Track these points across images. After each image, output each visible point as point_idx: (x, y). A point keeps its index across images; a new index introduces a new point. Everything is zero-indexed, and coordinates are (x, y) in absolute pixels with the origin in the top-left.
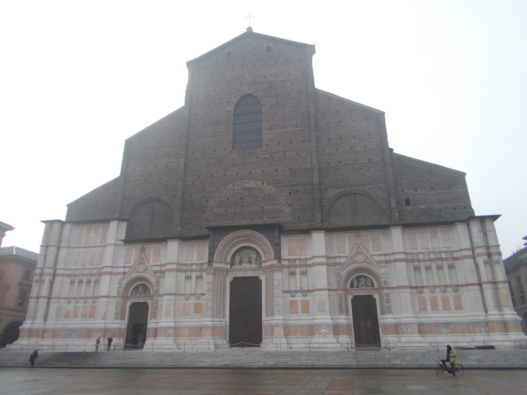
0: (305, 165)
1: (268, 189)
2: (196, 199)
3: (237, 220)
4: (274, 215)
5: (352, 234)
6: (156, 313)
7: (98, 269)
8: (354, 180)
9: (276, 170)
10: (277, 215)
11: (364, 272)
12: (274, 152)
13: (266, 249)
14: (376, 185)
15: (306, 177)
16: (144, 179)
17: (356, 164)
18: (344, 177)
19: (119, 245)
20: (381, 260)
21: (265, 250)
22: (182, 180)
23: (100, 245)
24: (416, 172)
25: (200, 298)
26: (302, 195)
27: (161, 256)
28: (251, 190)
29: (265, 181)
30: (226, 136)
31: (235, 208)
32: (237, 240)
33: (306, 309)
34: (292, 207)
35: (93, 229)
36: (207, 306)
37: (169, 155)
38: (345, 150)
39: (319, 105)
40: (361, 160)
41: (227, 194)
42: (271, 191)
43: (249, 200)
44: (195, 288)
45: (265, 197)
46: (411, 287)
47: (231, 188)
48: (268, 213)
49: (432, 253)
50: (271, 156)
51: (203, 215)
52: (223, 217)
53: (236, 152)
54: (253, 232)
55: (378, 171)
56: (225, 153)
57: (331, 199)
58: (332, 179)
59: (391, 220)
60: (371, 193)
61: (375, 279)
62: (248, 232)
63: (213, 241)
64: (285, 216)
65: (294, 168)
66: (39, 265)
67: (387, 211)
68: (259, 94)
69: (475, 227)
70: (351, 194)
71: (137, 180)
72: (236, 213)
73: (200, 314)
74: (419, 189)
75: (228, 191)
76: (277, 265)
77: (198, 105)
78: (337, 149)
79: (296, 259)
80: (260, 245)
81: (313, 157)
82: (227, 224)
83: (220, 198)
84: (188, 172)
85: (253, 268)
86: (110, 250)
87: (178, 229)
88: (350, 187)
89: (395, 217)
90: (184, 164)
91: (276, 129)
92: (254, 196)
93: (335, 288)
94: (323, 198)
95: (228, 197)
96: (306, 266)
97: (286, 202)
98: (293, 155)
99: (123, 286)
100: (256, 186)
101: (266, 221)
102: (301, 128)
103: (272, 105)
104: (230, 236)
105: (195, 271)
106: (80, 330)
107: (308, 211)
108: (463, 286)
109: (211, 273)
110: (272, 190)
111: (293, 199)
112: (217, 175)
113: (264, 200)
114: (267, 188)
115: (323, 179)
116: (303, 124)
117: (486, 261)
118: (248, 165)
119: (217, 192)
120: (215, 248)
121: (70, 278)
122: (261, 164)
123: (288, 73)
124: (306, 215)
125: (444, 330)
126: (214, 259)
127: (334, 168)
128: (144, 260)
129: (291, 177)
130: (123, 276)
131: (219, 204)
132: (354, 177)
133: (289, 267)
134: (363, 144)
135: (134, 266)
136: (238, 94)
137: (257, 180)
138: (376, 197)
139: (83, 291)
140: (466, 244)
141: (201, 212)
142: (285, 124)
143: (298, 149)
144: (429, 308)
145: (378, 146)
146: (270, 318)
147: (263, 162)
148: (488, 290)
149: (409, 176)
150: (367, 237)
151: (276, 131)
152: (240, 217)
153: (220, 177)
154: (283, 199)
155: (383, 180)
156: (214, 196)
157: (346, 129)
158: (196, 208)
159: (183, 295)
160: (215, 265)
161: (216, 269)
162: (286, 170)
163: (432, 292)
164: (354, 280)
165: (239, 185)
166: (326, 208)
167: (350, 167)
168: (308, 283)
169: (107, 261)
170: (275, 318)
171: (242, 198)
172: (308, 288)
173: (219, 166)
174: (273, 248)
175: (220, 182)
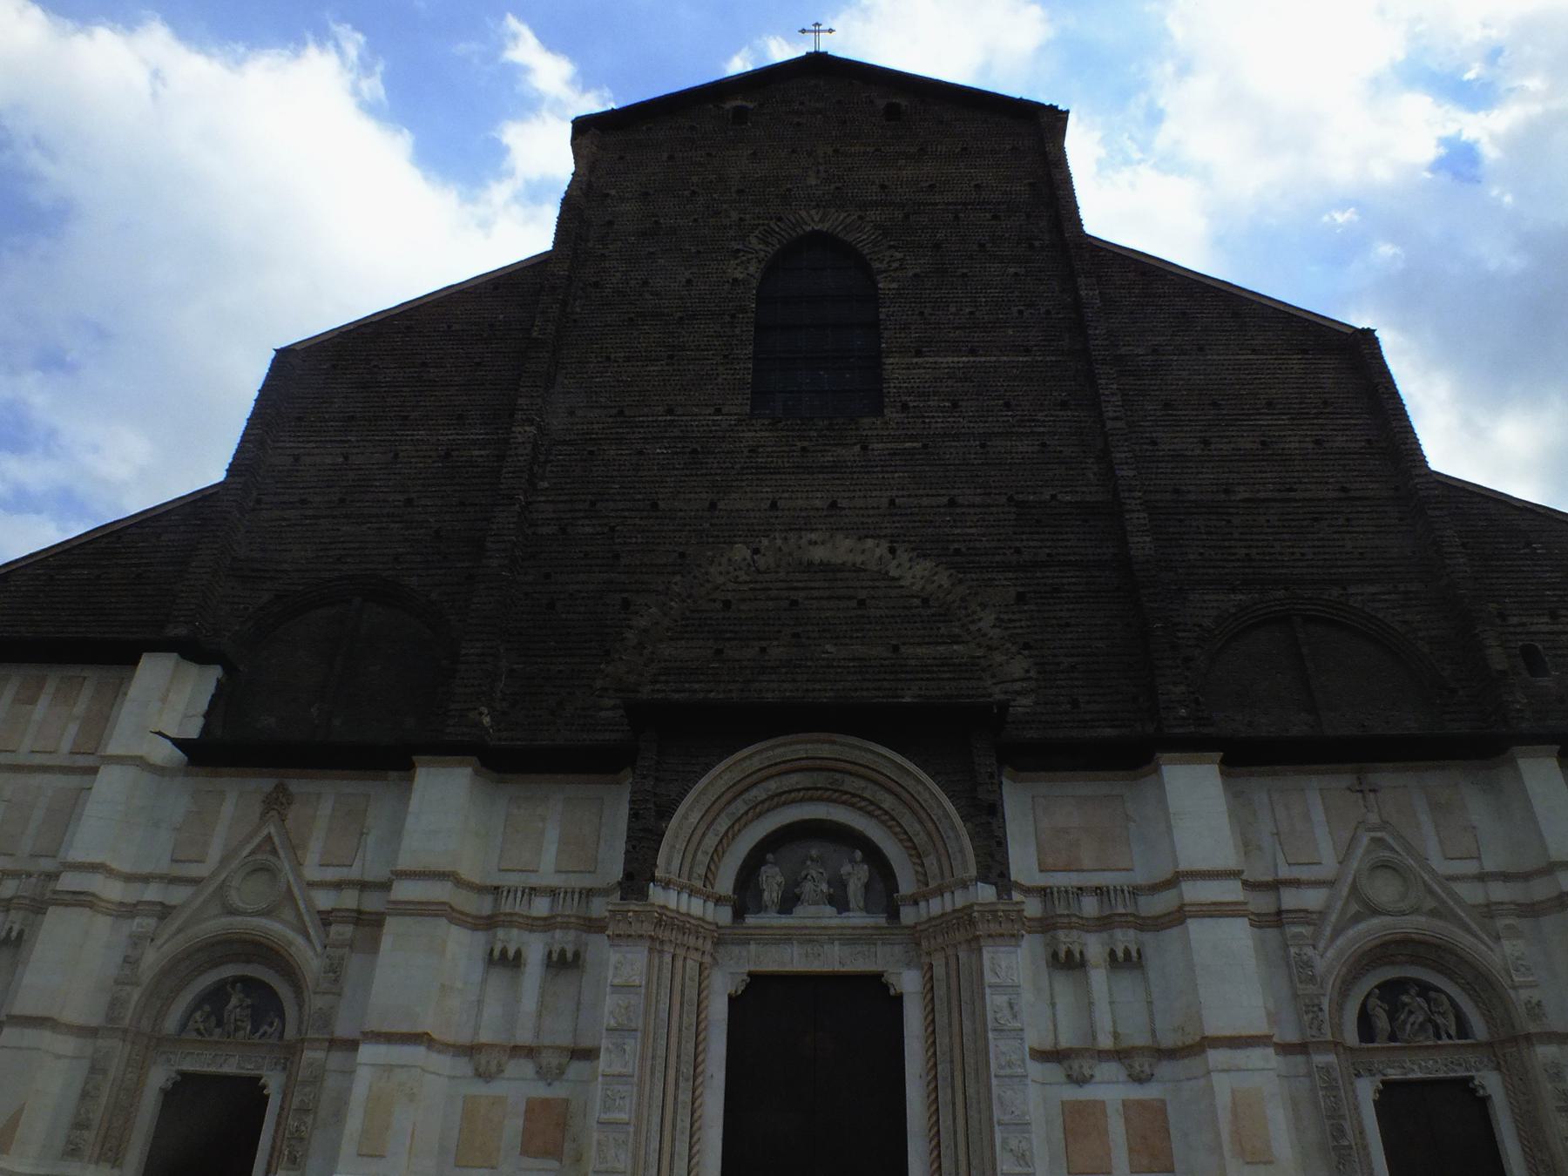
0: (1078, 489)
1: (915, 573)
2: (571, 594)
6: (302, 1139)
7: (33, 880)
8: (1294, 560)
9: (952, 503)
11: (1415, 960)
13: (929, 834)
17: (1295, 500)
18: (1250, 547)
21: (921, 839)
23: (66, 763)
24: (1536, 549)
25: (561, 1071)
28: (839, 575)
29: (904, 542)
31: (764, 644)
32: (773, 785)
34: (1036, 652)
35: (50, 688)
36: (604, 1117)
41: (724, 584)
42: (933, 582)
44: (540, 1015)
45: (905, 607)
47: (745, 559)
48: (921, 676)
50: (925, 446)
52: (701, 682)
54: (860, 748)
56: (719, 425)
58: (1202, 551)
60: (1380, 616)
64: (1006, 693)
65: (1031, 497)
71: (303, 502)
73: (555, 1164)
75: (728, 573)
79: (1080, 889)
80: (893, 819)
81: (1118, 455)
85: (854, 928)
88: (1286, 589)
90: (529, 447)
92: (854, 598)
93: (1292, 1037)
95: (729, 596)
98: (1021, 449)
100: (859, 559)
102: (1048, 359)
103: (916, 275)
104: (744, 759)
105: (546, 924)
109: (641, 936)
110: (936, 578)
113: (898, 620)
114: (910, 568)
118: (821, 476)
119: (674, 573)
120: (666, 812)
126: (655, 865)
127: (1204, 510)
128: (274, 852)
132: (1295, 550)
134: (1309, 433)
135: (223, 877)
137: (867, 537)
143: (1042, 429)
145: (1369, 441)
147: (889, 469)
149: (1515, 560)
151: (940, 360)
152: (786, 685)
154: (987, 620)
159: (470, 1051)
160: (656, 895)
161: (666, 920)
162: (997, 506)
164: (1373, 1001)
165: (780, 549)
167: (1272, 511)
168: (1151, 1015)
171: (794, 603)
172: (1153, 1032)
173: (688, 472)
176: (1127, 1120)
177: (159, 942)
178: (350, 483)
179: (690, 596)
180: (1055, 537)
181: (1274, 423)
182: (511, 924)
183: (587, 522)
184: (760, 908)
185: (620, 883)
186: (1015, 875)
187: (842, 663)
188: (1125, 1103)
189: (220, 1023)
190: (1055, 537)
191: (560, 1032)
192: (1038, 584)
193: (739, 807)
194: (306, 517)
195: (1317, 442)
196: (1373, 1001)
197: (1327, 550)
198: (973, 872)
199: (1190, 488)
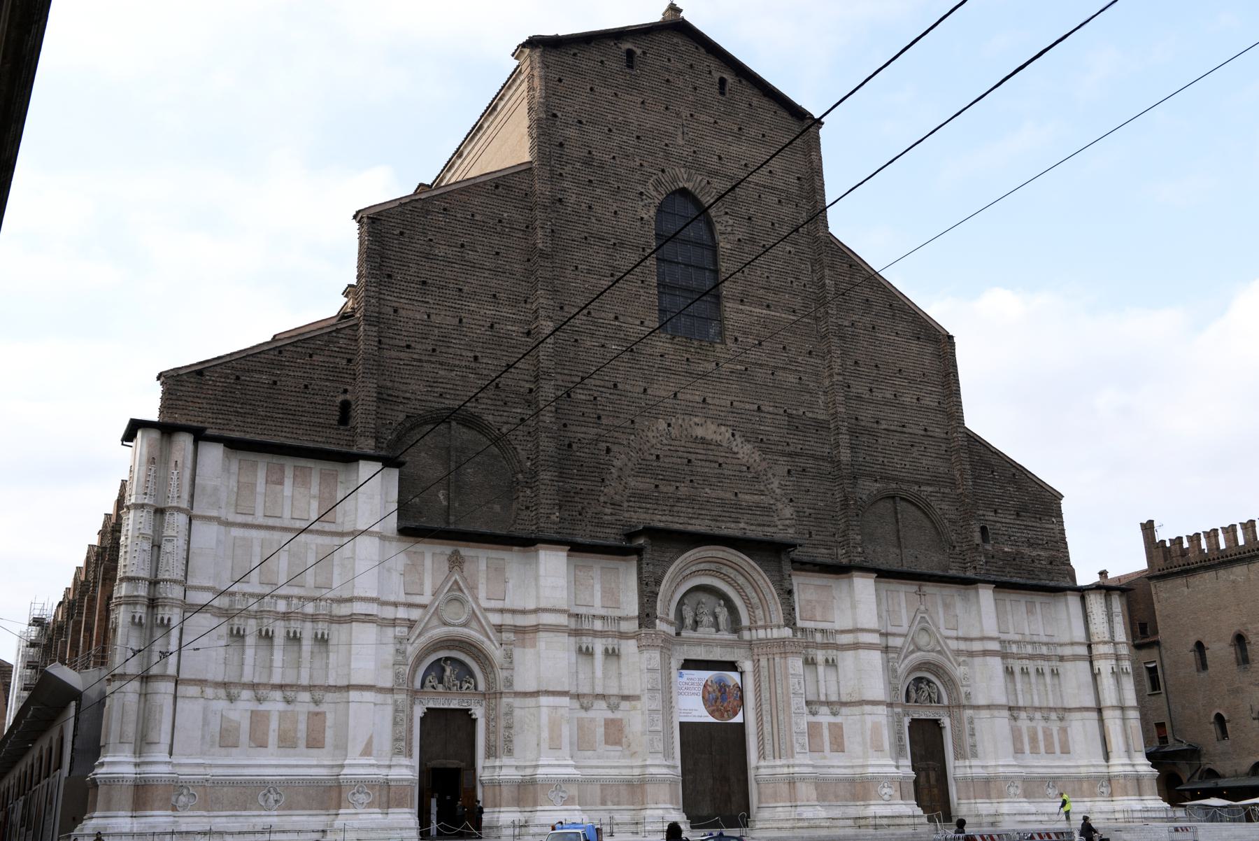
3: (682, 515)
5: (912, 587)
10: (766, 518)
11: (928, 670)
12: (753, 364)
16: (430, 348)
17: (905, 433)
20: (960, 648)
21: (755, 600)
26: (813, 481)
27: (510, 585)
28: (710, 447)
31: (678, 484)
33: (838, 744)
35: (289, 472)
36: (651, 729)
38: (885, 396)
43: (706, 470)
48: (747, 511)
50: (746, 369)
51: (602, 488)
53: (669, 336)
54: (735, 555)
62: (725, 554)
65: (794, 412)
67: (957, 548)
73: (620, 748)
74: (1000, 511)
75: (657, 437)
77: (564, 175)
78: (871, 390)
83: (640, 449)
91: (753, 305)
93: (888, 701)
99: (410, 661)
100: (719, 438)
103: (739, 240)
107: (826, 521)
111: (796, 488)
112: (628, 387)
114: (742, 447)
120: (658, 582)
122: (727, 385)
124: (822, 529)
125: (1050, 790)
128: (461, 590)
130: (406, 630)
131: (639, 466)
135: (436, 604)
140: (1080, 635)
141: (597, 479)
143: (801, 369)
144: (1027, 748)
145: (939, 403)
151: (753, 309)
152: (689, 510)
153: (636, 395)
158: (582, 465)
159: (578, 696)
168: (838, 686)
169: (366, 585)
170: (797, 762)
171: (689, 461)
172: (839, 694)
173: (630, 365)
176: (830, 731)
177: (411, 641)
178: (436, 338)
182: (586, 635)
183: (582, 392)
187: (713, 500)
188: (829, 723)
195: (918, 399)
196: (911, 687)
199: (864, 418)
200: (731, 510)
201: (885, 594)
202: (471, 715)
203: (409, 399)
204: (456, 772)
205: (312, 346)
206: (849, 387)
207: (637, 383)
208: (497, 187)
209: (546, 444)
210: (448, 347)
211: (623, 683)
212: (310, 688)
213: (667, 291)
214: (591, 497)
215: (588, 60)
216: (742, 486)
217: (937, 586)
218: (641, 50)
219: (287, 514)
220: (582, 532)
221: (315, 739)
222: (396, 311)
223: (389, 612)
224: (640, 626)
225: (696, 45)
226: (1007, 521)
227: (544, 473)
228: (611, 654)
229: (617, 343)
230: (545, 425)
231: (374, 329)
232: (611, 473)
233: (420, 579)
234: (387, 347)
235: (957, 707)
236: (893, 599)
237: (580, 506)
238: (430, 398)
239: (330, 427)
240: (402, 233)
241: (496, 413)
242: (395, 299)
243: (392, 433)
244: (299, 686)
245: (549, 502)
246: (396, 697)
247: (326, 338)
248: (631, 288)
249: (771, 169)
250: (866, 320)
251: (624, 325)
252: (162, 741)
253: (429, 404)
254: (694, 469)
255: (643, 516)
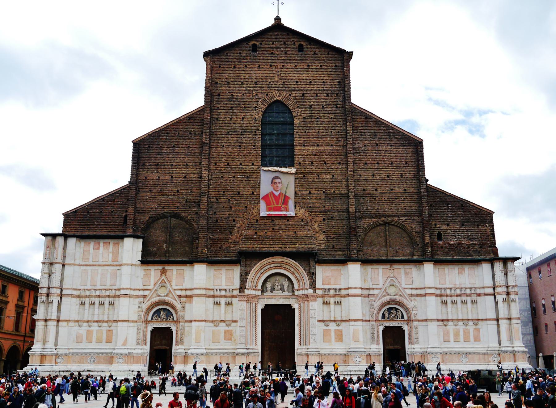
2: (221, 218)
3: (267, 244)
4: (308, 241)
7: (113, 291)
9: (310, 193)
13: (300, 277)
14: (411, 218)
15: (341, 203)
17: (392, 193)
19: (135, 265)
21: (299, 278)
22: (206, 196)
25: (230, 325)
27: (186, 279)
30: (253, 149)
31: (266, 231)
32: (269, 266)
33: (339, 338)
35: (102, 244)
37: (187, 165)
38: (382, 177)
39: (356, 124)
40: (397, 189)
46: (438, 320)
49: (459, 288)
50: (304, 176)
55: (413, 202)
57: (366, 229)
59: (423, 254)
60: (406, 225)
61: (406, 311)
63: (245, 267)
65: (329, 192)
66: (44, 284)
67: (420, 245)
68: (291, 103)
69: (498, 266)
70: (385, 224)
71: (150, 191)
72: (266, 237)
73: (231, 342)
74: (451, 224)
76: (313, 295)
78: (373, 175)
82: (256, 248)
84: (211, 186)
86: (126, 270)
87: (204, 251)
88: (385, 218)
89: (428, 253)
91: (310, 146)
93: (368, 319)
94: (358, 227)
95: (258, 219)
96: (341, 296)
97: (320, 229)
99: (144, 311)
101: (299, 247)
103: (304, 118)
105: (225, 296)
106: (98, 355)
107: (343, 239)
108: (482, 320)
115: (359, 207)
116: (339, 143)
117: (505, 300)
119: (245, 212)
120: (247, 274)
121: (78, 299)
123: (323, 81)
125: (463, 359)
128: (165, 283)
129: (326, 202)
132: (389, 207)
133: (323, 296)
135: (155, 289)
136: (267, 99)
138: (410, 230)
139: (97, 313)
140: (489, 283)
142: (319, 141)
143: (333, 171)
144: (452, 339)
145: (415, 175)
146: (304, 347)
148: (504, 324)
150: (401, 271)
151: (309, 148)
152: (271, 241)
154: (316, 225)
155: (417, 213)
156: (242, 216)
157: (384, 155)
159: (213, 321)
160: (247, 292)
161: (250, 297)
163: (456, 325)
166: (360, 237)
168: (341, 313)
172: (342, 317)
173: (246, 183)
174: (309, 277)
175: (248, 201)
176: (335, 333)
177: (145, 303)
179: (249, 218)
180: (333, 203)
181: (392, 169)
184: (267, 291)
185: (239, 289)
186: (318, 286)
187: (283, 236)
188: (335, 330)
189: (159, 317)
190: (333, 203)
191: (229, 318)
192: (328, 216)
193: (262, 271)
194: (153, 195)
197: (397, 207)
198: (309, 287)
200: (292, 239)
201: (370, 270)
202: (171, 329)
203: (150, 211)
204: (165, 350)
205: (115, 196)
206: (361, 176)
207: (249, 190)
208: (189, 119)
209: (202, 222)
210: (166, 188)
211: (233, 315)
212: (107, 321)
213: (268, 147)
214: (225, 241)
215: (233, 55)
216: (299, 228)
217: (401, 265)
218: (259, 43)
219: (100, 260)
220: (220, 256)
221: (108, 339)
222: (146, 178)
223: (137, 293)
224: (240, 293)
225: (287, 32)
226: (455, 228)
227: (201, 234)
228: (228, 304)
229: (240, 175)
230: (202, 214)
231: (134, 187)
232: (234, 230)
233: (149, 280)
234: (142, 192)
235: (410, 321)
236: (374, 273)
237: (220, 245)
238: (158, 209)
239: (120, 225)
240: (149, 147)
241: (185, 212)
242: (145, 173)
243: (143, 225)
244: (103, 321)
245: (202, 245)
246: (138, 324)
247: (120, 192)
248: (248, 150)
249: (324, 81)
250: (373, 142)
251: (244, 166)
252: (50, 340)
253: (158, 212)
254: (274, 223)
255: (248, 246)
